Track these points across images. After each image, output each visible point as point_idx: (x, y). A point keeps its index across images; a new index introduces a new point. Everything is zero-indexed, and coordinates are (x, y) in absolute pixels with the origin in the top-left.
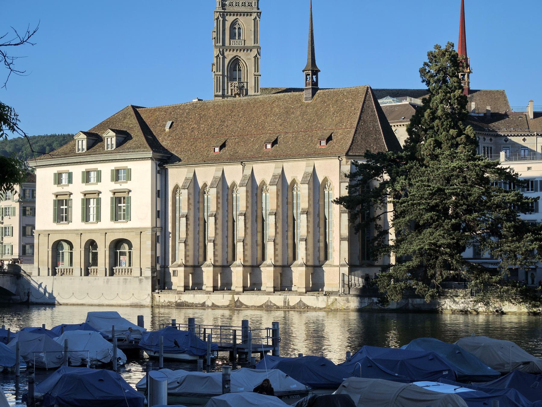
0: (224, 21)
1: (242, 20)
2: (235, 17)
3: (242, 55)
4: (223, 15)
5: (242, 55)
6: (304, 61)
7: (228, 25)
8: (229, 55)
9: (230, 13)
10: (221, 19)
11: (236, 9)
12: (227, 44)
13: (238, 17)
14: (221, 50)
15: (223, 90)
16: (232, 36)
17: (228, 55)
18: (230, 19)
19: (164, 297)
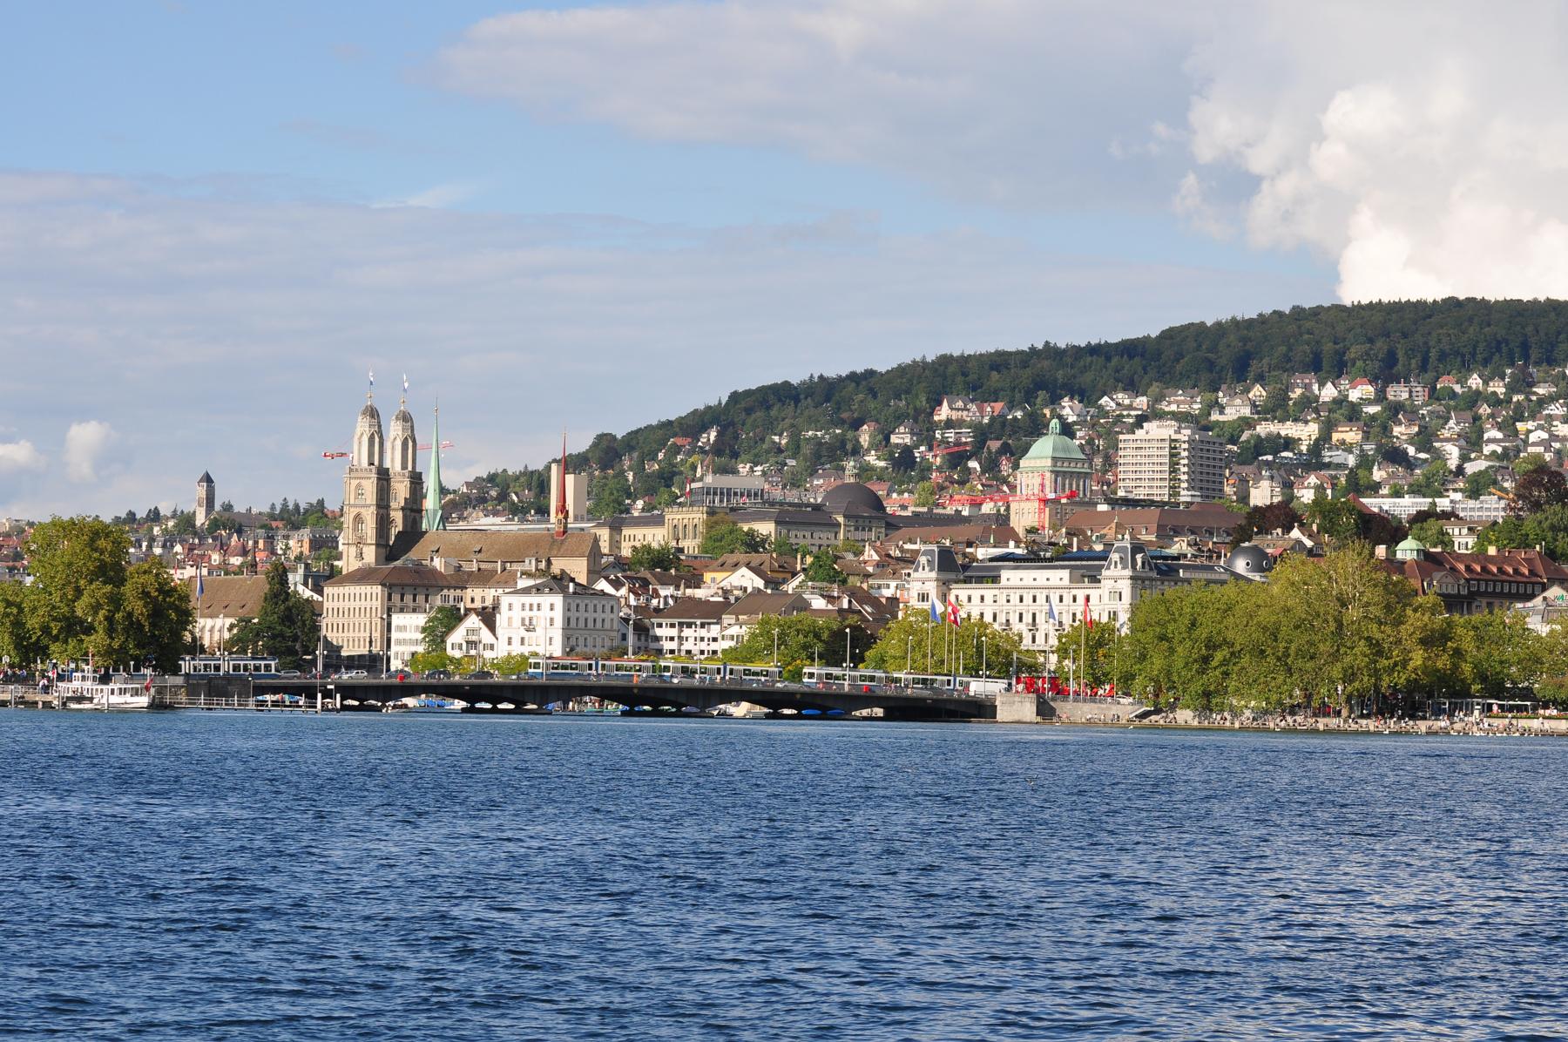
1: (364, 482)
3: (363, 510)
5: (363, 510)
18: (354, 482)
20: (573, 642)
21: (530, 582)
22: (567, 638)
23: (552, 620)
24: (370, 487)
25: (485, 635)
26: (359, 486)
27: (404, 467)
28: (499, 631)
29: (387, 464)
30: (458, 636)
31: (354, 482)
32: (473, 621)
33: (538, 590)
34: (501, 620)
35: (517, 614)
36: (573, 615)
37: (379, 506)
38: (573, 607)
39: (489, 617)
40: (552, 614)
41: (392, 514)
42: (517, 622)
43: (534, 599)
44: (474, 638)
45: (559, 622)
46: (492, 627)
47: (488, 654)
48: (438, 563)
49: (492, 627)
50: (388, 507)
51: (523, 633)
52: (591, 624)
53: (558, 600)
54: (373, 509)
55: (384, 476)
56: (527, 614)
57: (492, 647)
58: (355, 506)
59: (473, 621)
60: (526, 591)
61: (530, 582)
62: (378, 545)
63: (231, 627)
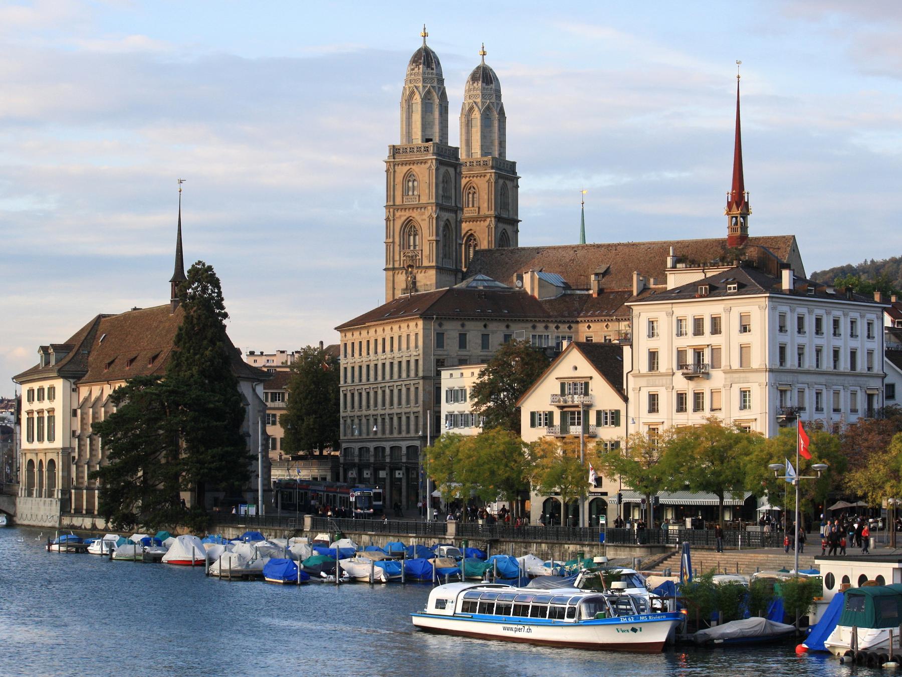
0: (395, 171)
2: (408, 167)
3: (415, 214)
4: (394, 166)
5: (415, 214)
6: (171, 273)
8: (402, 216)
9: (403, 163)
10: (392, 170)
11: (408, 157)
12: (398, 201)
13: (412, 166)
14: (391, 210)
15: (394, 261)
16: (405, 193)
17: (400, 216)
18: (402, 170)
19: (66, 521)
20: (791, 401)
21: (696, 276)
22: (780, 391)
23: (744, 350)
24: (425, 175)
25: (602, 395)
26: (409, 177)
27: (485, 151)
28: (631, 384)
29: (454, 140)
30: (542, 398)
31: (402, 170)
32: (574, 364)
33: (713, 289)
34: (634, 360)
35: (666, 346)
36: (792, 339)
37: (440, 207)
38: (791, 324)
39: (608, 360)
40: (745, 338)
41: (465, 227)
42: (666, 362)
43: (706, 309)
44: (577, 399)
45: (760, 356)
47: (608, 433)
48: (528, 283)
50: (457, 210)
51: (681, 383)
52: (827, 363)
53: (757, 308)
54: (431, 211)
55: (447, 159)
56: (690, 341)
57: (615, 419)
58: (404, 208)
59: (574, 364)
60: (686, 293)
61: (696, 276)
62: (439, 269)
63: (117, 397)
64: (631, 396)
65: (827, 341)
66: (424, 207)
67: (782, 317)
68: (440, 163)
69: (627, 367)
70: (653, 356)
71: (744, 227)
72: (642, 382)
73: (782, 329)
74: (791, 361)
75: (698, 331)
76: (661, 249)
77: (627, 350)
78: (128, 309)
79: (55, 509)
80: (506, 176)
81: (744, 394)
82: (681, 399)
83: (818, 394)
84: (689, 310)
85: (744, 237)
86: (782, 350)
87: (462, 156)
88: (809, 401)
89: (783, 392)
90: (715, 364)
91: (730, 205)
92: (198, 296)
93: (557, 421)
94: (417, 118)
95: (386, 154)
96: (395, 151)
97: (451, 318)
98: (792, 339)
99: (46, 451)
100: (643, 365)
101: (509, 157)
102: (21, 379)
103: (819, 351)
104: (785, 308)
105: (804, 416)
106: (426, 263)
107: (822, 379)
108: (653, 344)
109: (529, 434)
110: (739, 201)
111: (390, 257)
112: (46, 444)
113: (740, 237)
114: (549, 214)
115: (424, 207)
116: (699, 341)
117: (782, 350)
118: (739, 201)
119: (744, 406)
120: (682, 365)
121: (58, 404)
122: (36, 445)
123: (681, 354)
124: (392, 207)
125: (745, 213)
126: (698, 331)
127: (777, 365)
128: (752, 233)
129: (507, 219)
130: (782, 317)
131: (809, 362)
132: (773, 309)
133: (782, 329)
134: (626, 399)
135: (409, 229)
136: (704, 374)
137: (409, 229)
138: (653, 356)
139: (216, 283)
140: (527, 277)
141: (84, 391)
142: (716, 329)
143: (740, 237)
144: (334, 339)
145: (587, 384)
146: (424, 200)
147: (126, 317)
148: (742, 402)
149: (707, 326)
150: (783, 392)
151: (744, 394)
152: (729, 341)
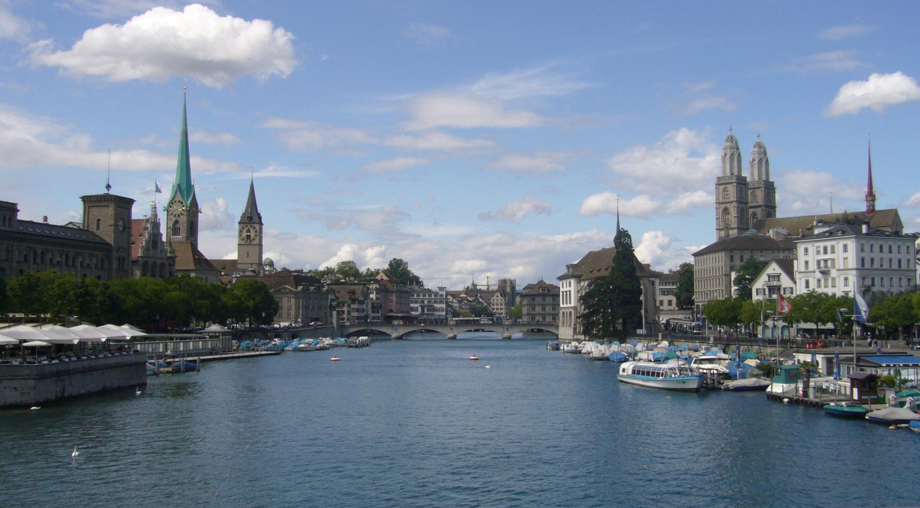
3: (728, 205)
7: (721, 190)
8: (723, 206)
20: (868, 282)
24: (732, 190)
25: (785, 281)
26: (725, 190)
28: (797, 276)
30: (761, 282)
31: (722, 187)
32: (774, 268)
33: (831, 234)
35: (812, 258)
38: (867, 248)
40: (846, 255)
42: (812, 266)
44: (775, 283)
45: (852, 263)
46: (790, 273)
49: (790, 273)
54: (735, 204)
55: (741, 182)
56: (822, 257)
58: (723, 203)
59: (774, 268)
60: (821, 236)
62: (739, 228)
64: (797, 281)
65: (886, 255)
66: (732, 202)
67: (862, 245)
68: (738, 183)
69: (795, 269)
70: (807, 263)
71: (874, 206)
72: (802, 275)
73: (862, 250)
74: (867, 265)
75: (825, 252)
76: (812, 218)
77: (795, 262)
78: (600, 249)
79: (572, 331)
80: (770, 188)
81: (846, 279)
82: (819, 281)
83: (882, 279)
84: (821, 245)
85: (873, 210)
86: (863, 260)
87: (748, 180)
88: (877, 281)
89: (864, 278)
90: (833, 266)
91: (867, 197)
92: (623, 242)
93: (767, 292)
94: (728, 165)
95: (715, 181)
96: (719, 178)
97: (735, 249)
98: (867, 256)
99: (568, 308)
100: (803, 269)
101: (771, 180)
102: (561, 278)
103: (891, 260)
104: (864, 242)
105: (875, 289)
106: (733, 226)
107: (883, 272)
108: (806, 258)
109: (755, 297)
110: (871, 196)
111: (718, 224)
112: (569, 305)
113: (871, 210)
114: (790, 205)
115: (732, 202)
116: (826, 257)
117: (863, 260)
118: (871, 196)
119: (846, 285)
120: (819, 267)
121: (572, 289)
122: (565, 306)
123: (819, 262)
124: (718, 203)
125: (873, 200)
126: (825, 252)
127: (860, 266)
128: (877, 208)
129: (770, 207)
130: (862, 245)
131: (876, 265)
132: (857, 242)
133: (862, 250)
134: (795, 283)
135: (726, 211)
136: (831, 270)
137: (726, 211)
138: (807, 263)
139: (629, 237)
140: (771, 231)
141: (582, 284)
142: (833, 252)
143: (871, 210)
144: (691, 260)
145: (779, 276)
146: (731, 200)
147: (599, 252)
148: (844, 284)
149: (829, 250)
150: (864, 278)
151: (846, 279)
152: (839, 255)
